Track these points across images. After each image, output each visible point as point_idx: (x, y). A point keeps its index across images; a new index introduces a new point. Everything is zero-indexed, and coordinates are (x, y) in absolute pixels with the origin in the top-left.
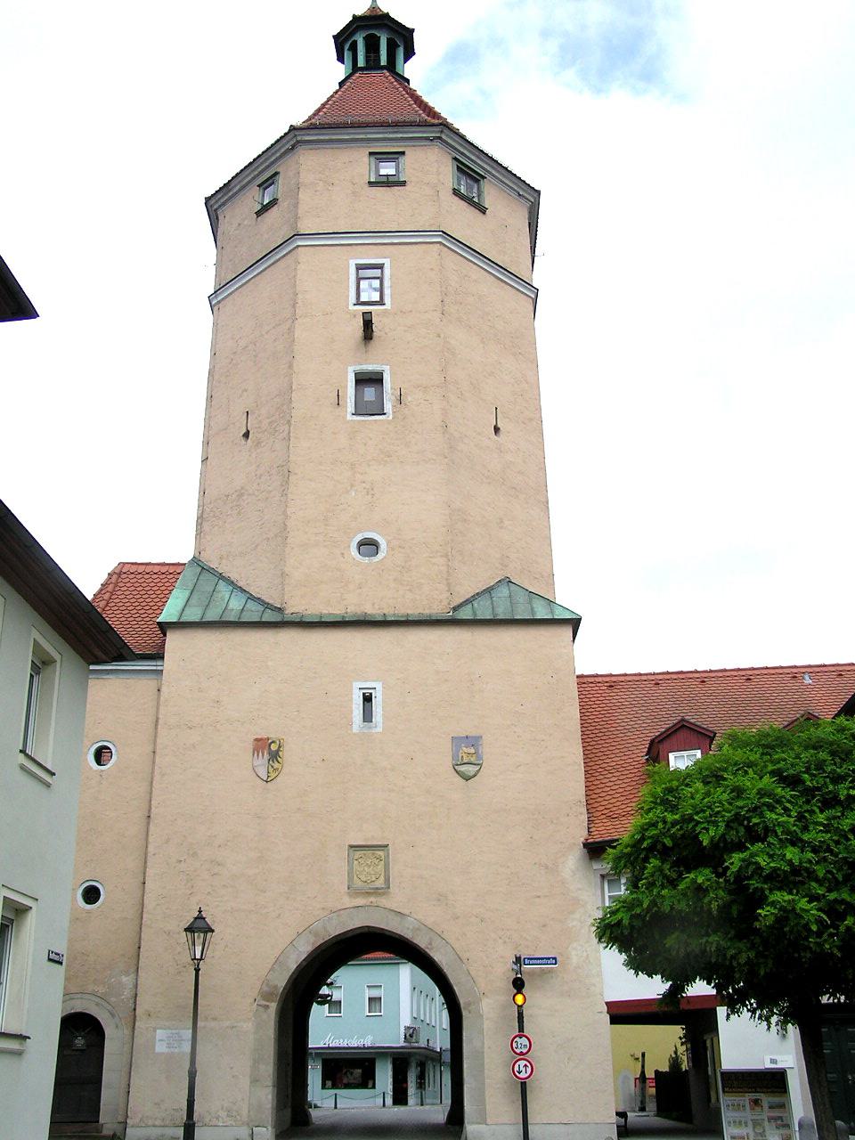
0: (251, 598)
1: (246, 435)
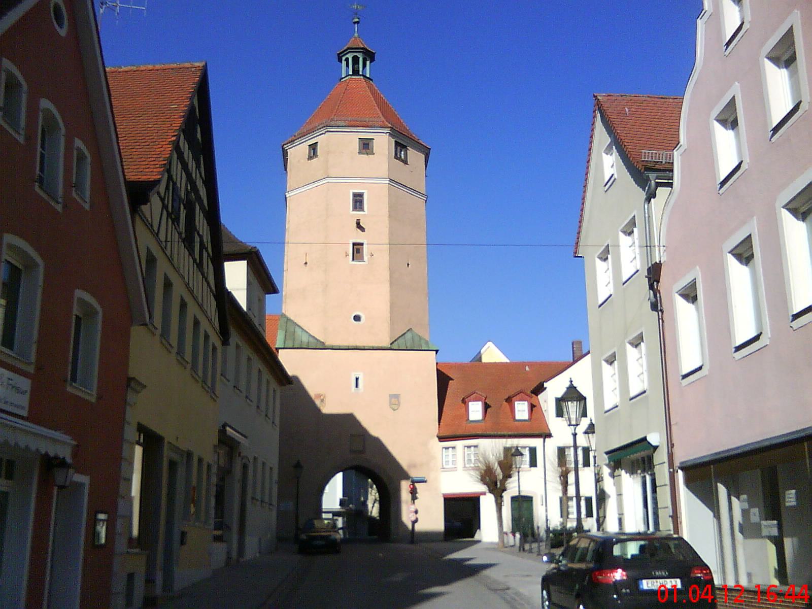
0: (310, 335)
1: (306, 263)
